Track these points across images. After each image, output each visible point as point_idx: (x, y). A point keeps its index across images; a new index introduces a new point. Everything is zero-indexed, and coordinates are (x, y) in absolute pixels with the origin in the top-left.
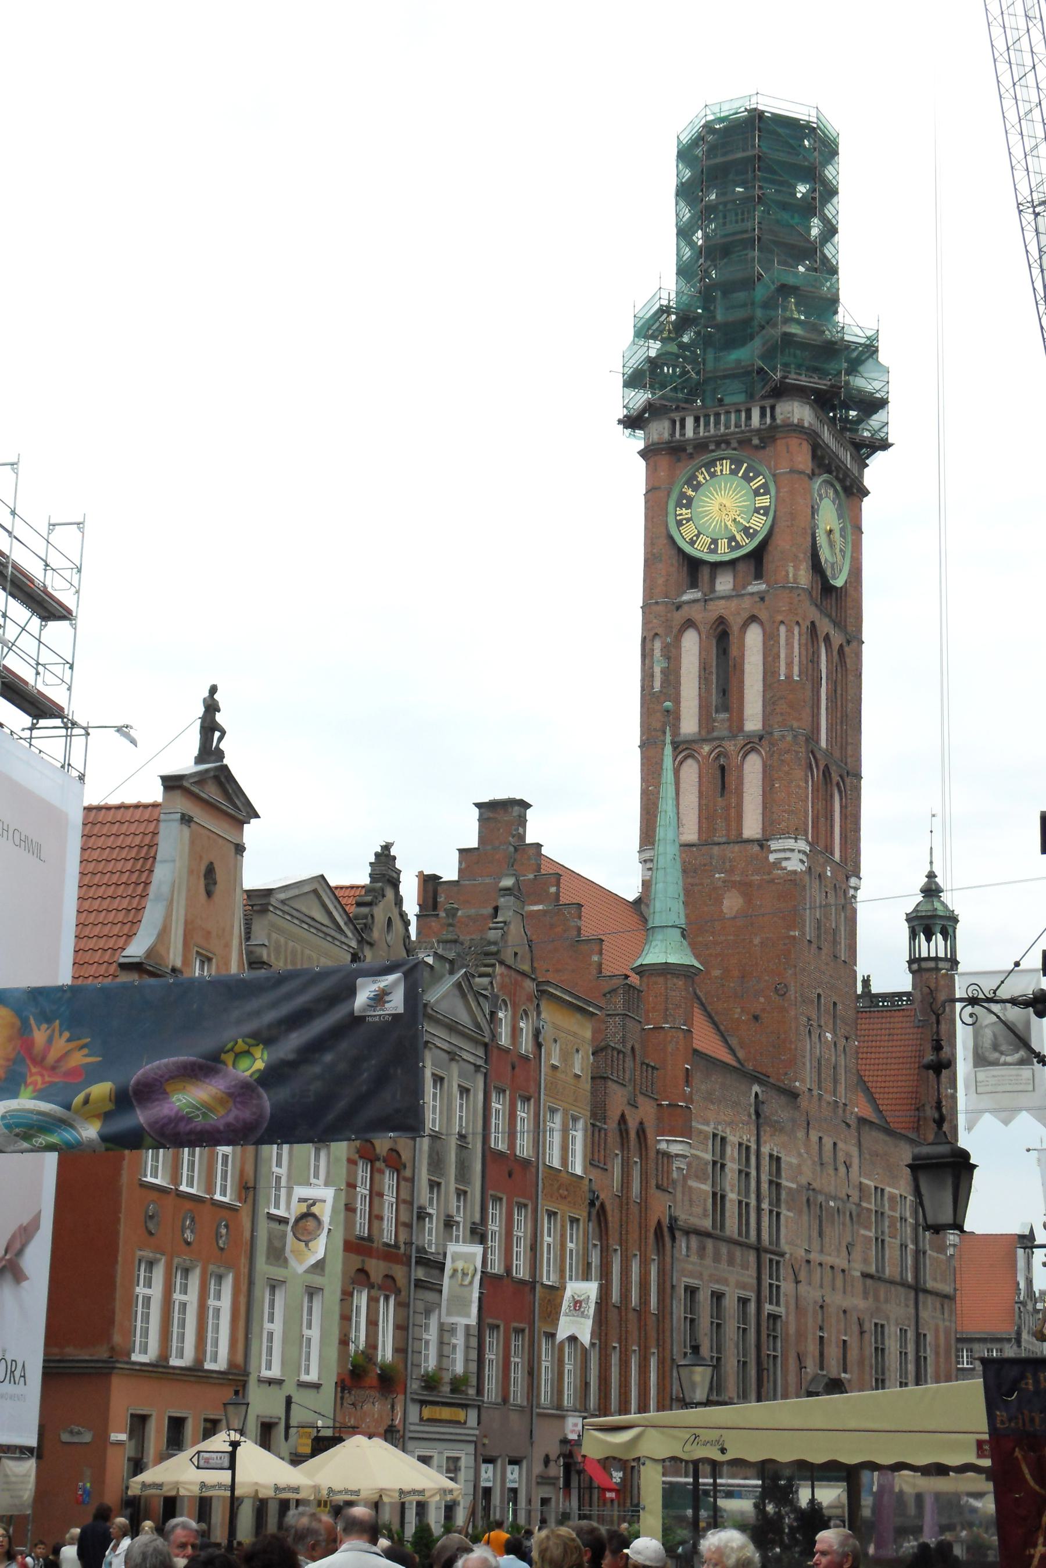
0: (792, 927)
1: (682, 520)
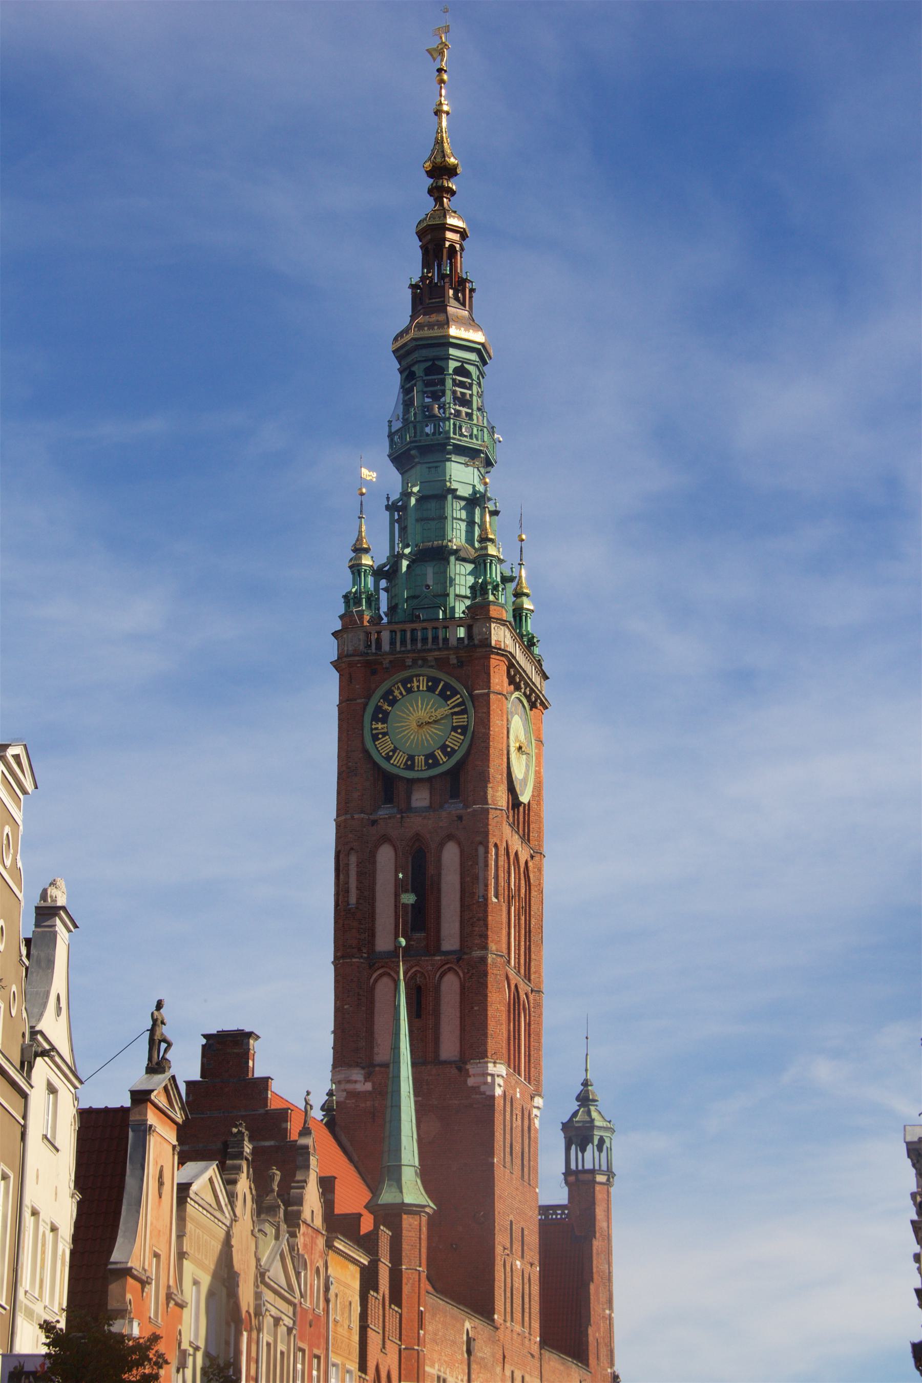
1: (378, 734)
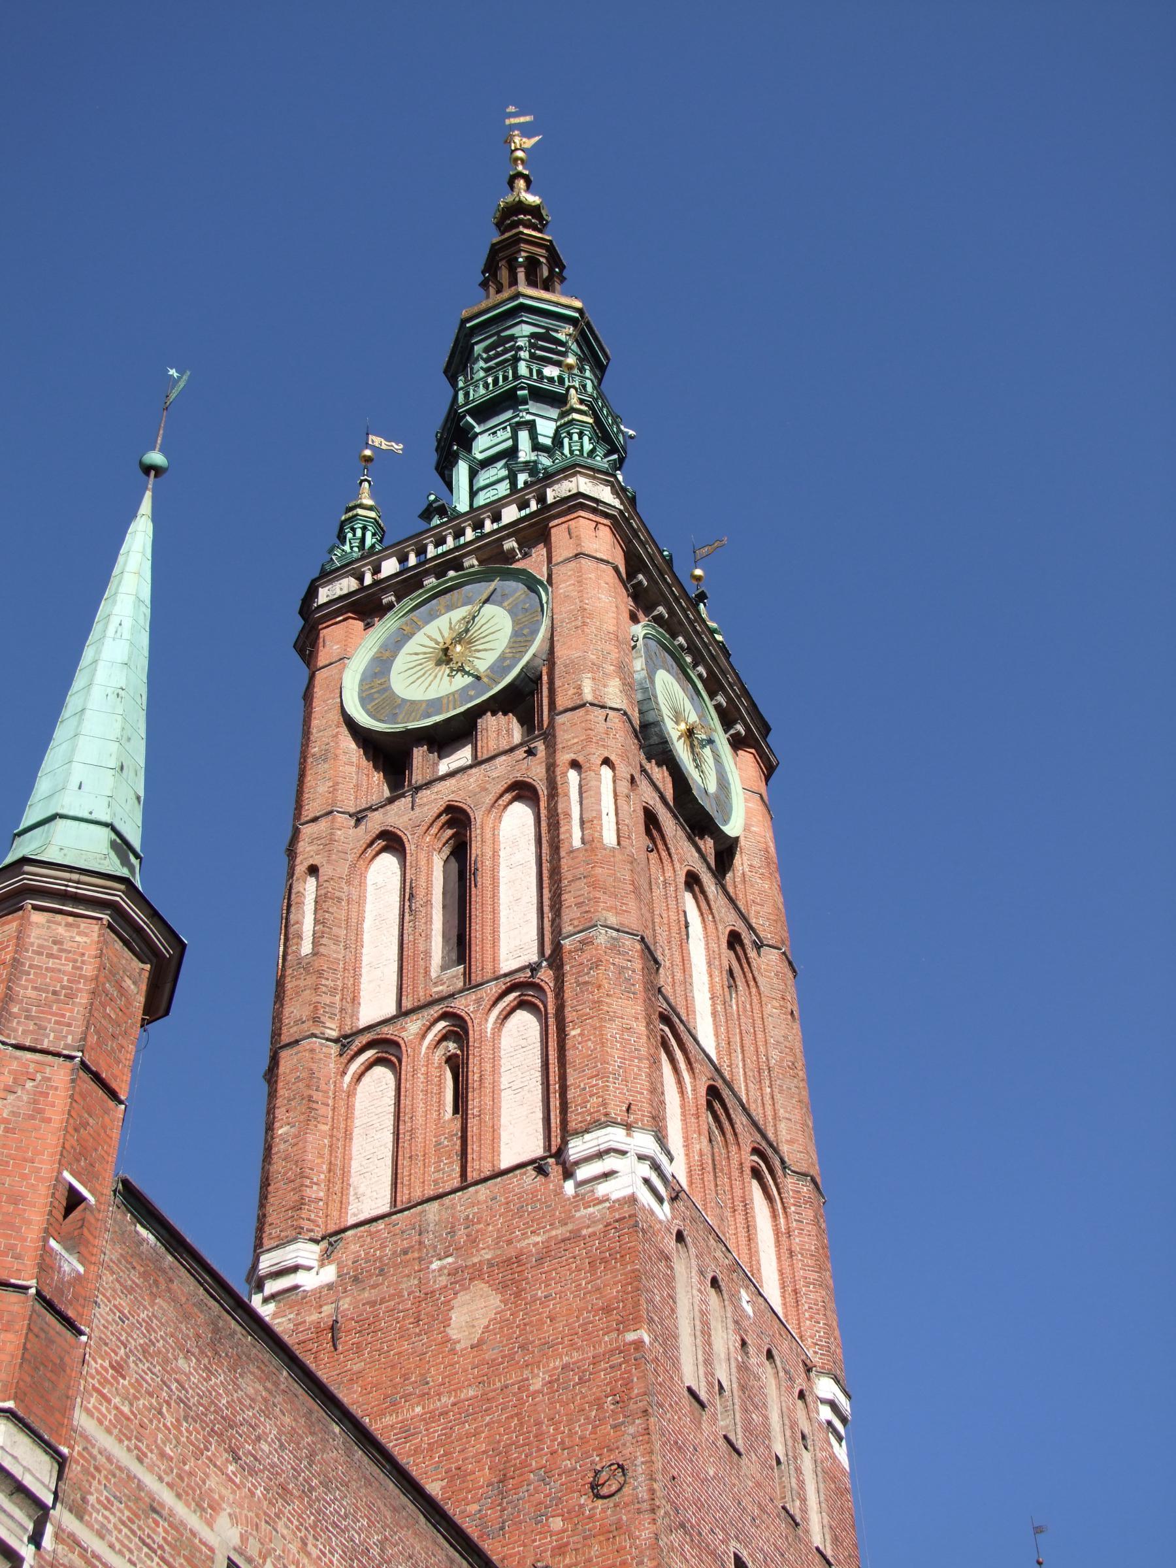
0: (632, 1320)
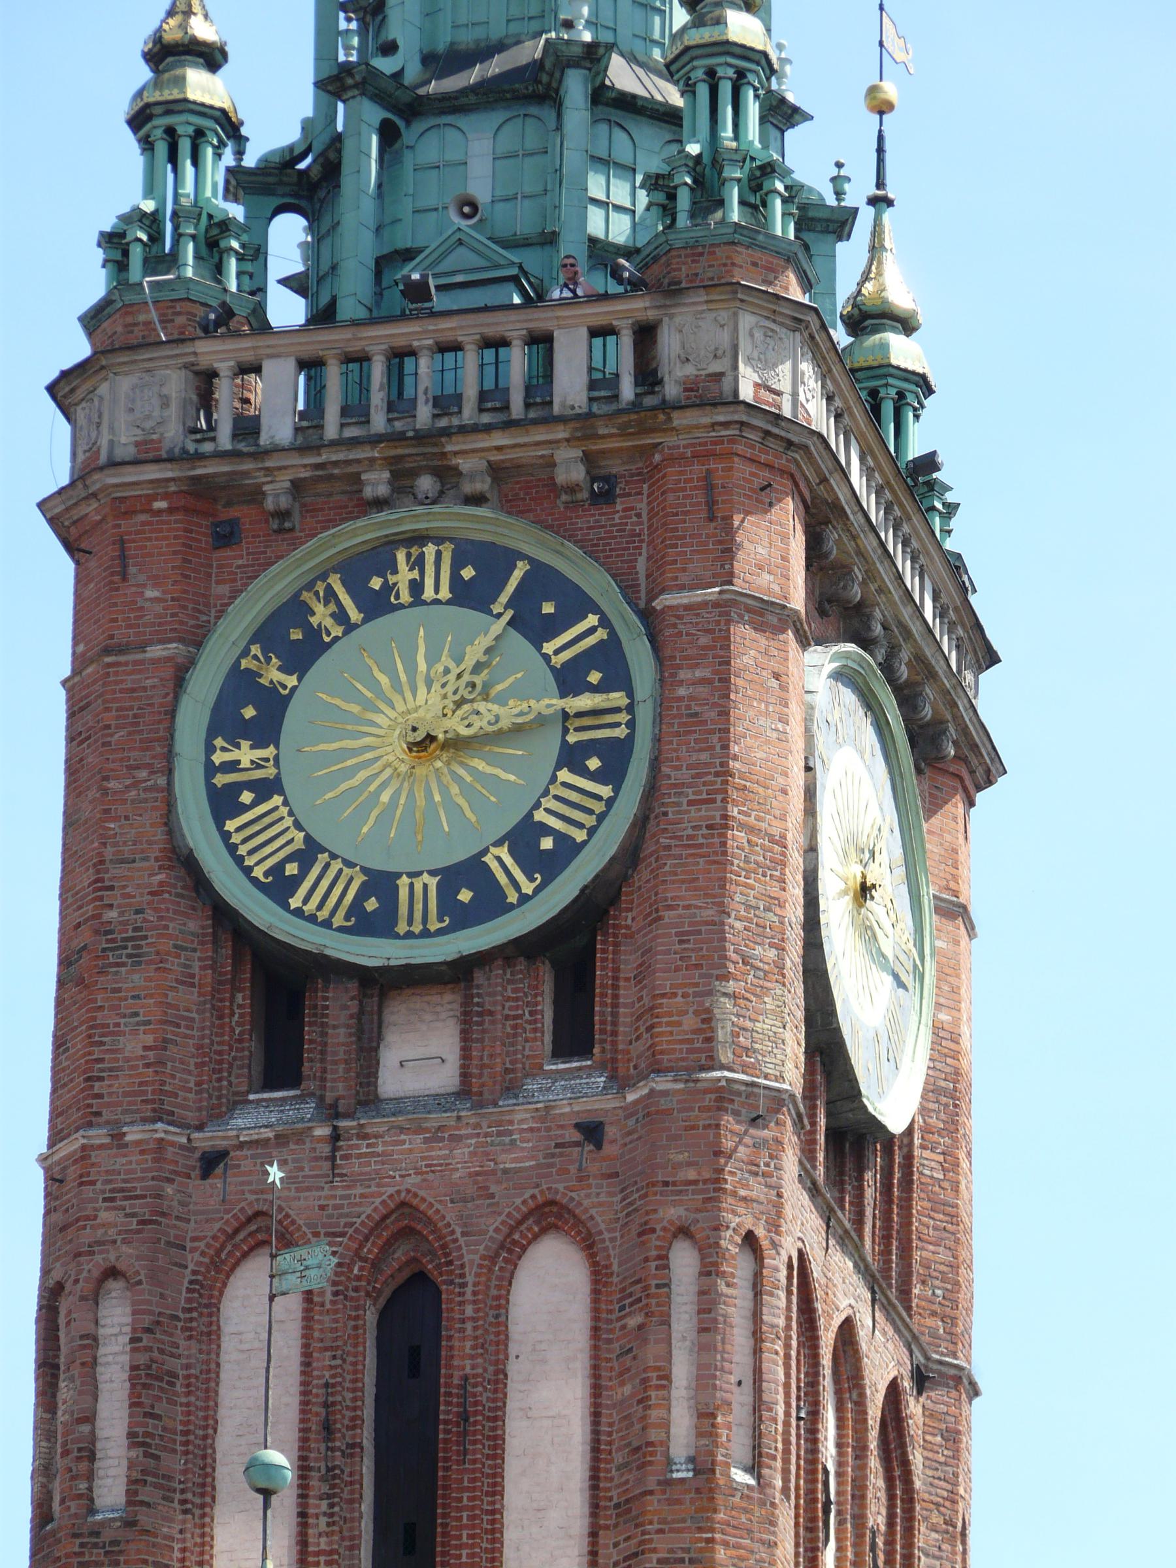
1: (238, 787)
